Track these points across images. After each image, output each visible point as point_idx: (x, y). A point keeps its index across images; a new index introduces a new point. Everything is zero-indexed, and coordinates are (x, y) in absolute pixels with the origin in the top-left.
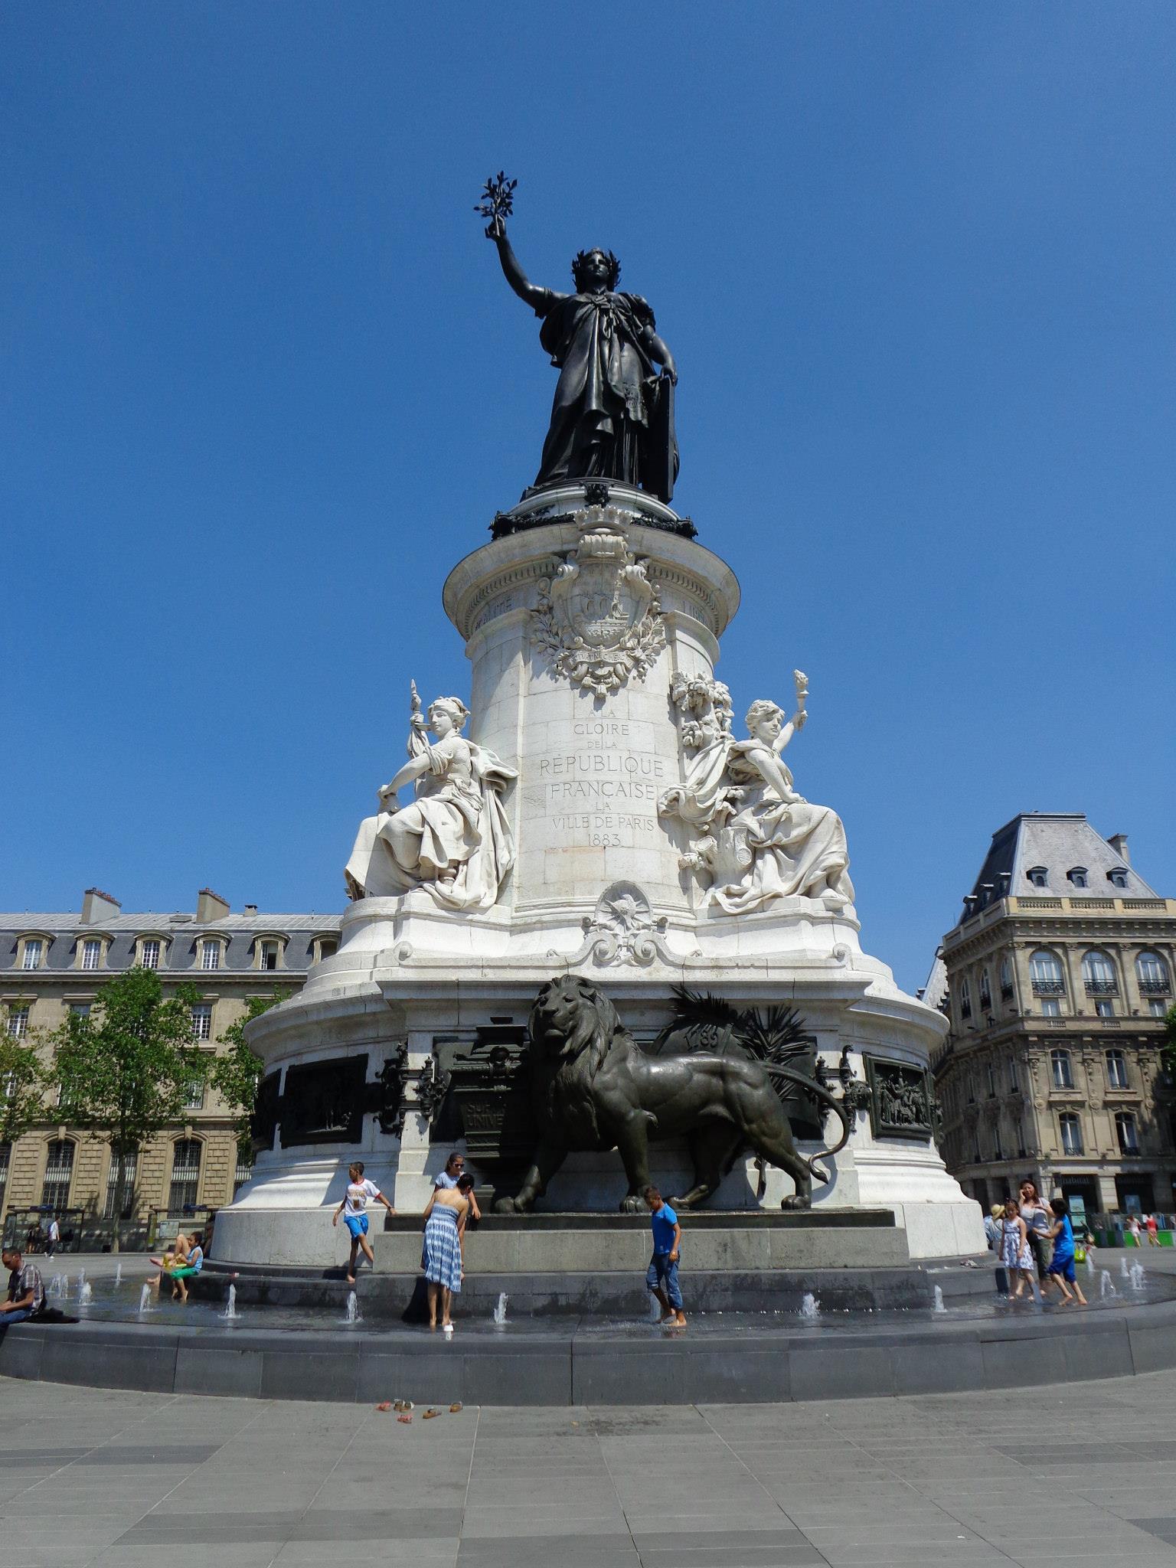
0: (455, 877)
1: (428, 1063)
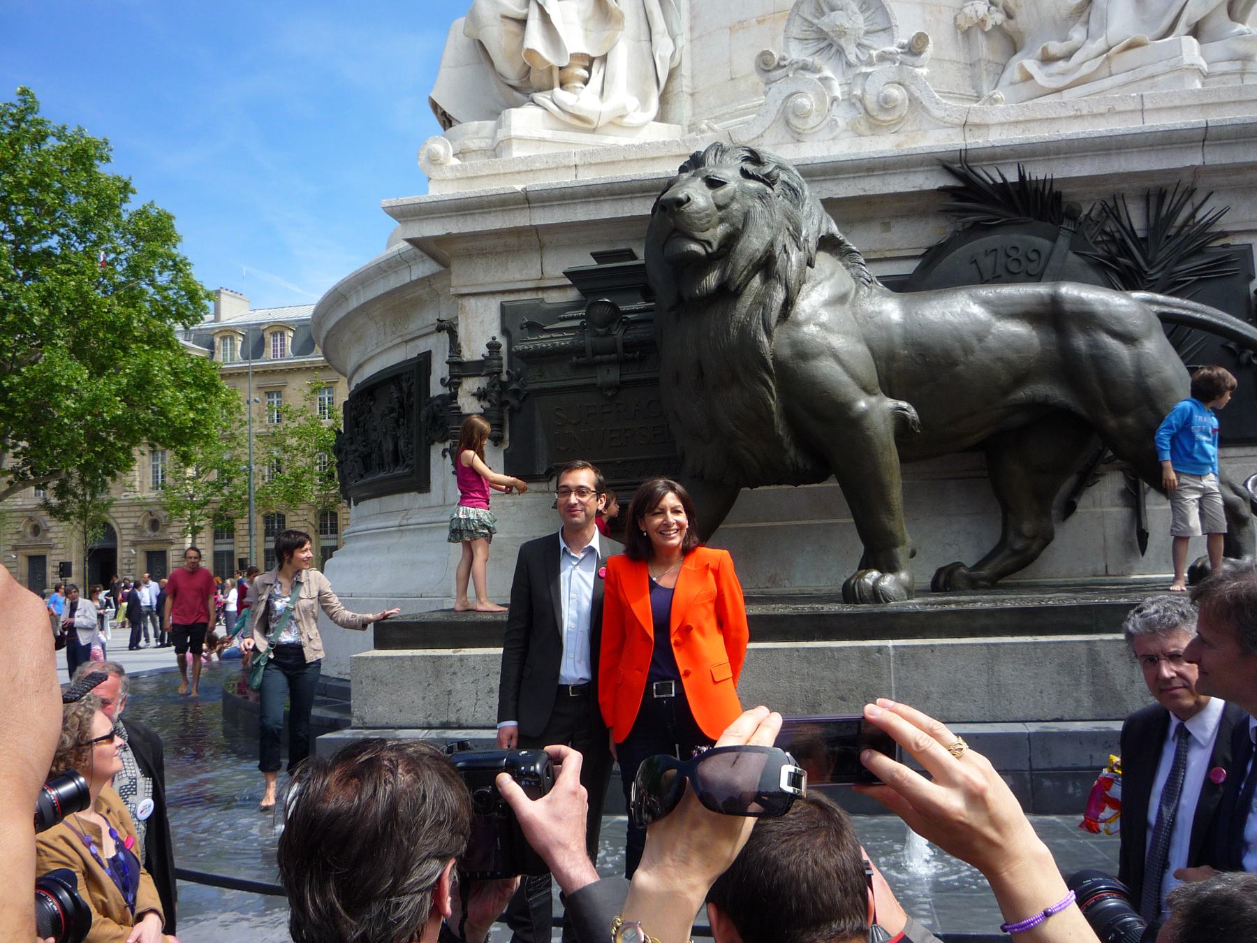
0: (586, 82)
1: (493, 347)
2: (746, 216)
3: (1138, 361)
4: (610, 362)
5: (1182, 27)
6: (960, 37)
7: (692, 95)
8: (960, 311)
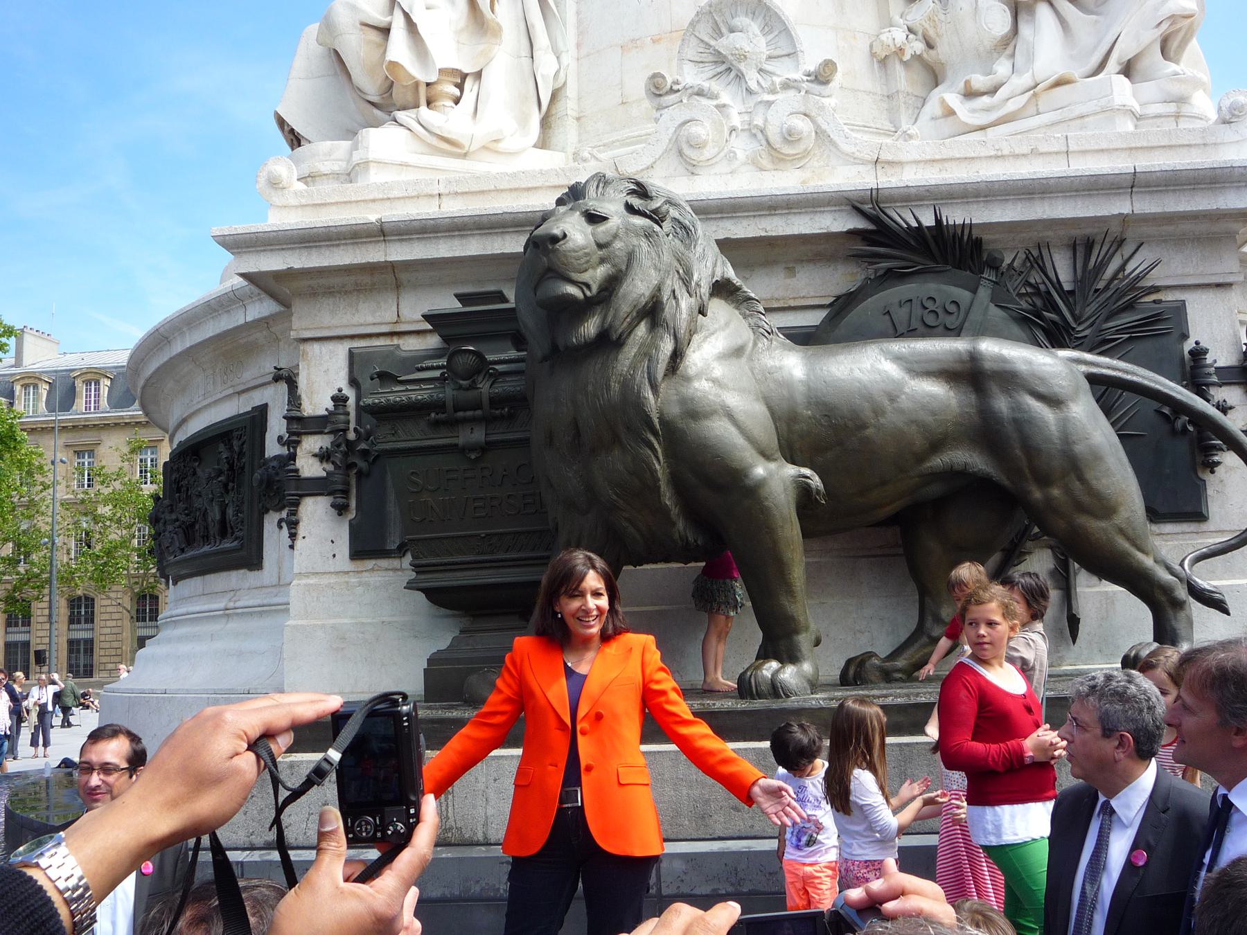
0: (457, 101)
1: (339, 400)
2: (631, 257)
3: (1064, 423)
4: (474, 420)
5: (1113, 65)
6: (876, 65)
7: (578, 119)
8: (872, 369)
